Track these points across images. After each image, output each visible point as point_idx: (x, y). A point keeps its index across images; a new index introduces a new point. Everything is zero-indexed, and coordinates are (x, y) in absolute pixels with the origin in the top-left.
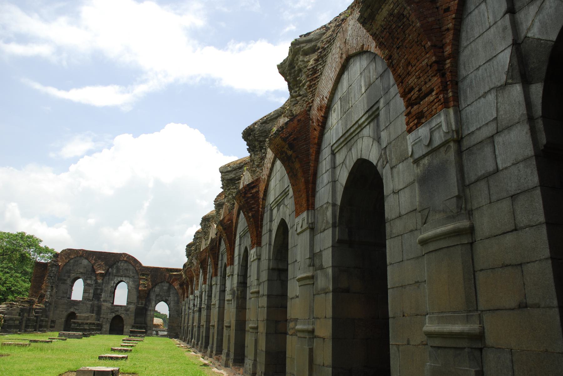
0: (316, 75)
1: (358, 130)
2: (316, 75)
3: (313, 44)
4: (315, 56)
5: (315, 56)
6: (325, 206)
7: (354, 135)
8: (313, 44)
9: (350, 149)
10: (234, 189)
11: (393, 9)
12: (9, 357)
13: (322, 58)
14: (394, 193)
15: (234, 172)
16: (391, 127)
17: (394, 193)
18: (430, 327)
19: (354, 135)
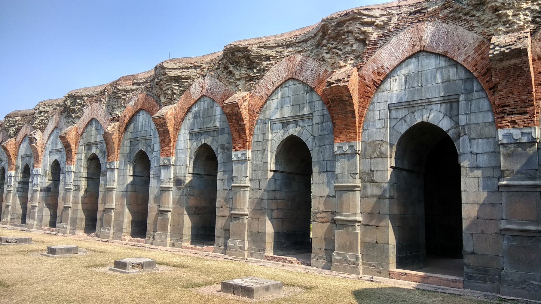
0: (375, 47)
1: (427, 104)
2: (375, 47)
3: (373, 19)
4: (381, 32)
5: (381, 32)
6: (378, 142)
7: (420, 105)
8: (373, 19)
9: (413, 112)
10: (176, 86)
11: (519, 64)
12: (86, 264)
13: (385, 36)
14: (471, 153)
15: (181, 71)
16: (472, 117)
17: (471, 153)
18: (504, 225)
19: (420, 105)
